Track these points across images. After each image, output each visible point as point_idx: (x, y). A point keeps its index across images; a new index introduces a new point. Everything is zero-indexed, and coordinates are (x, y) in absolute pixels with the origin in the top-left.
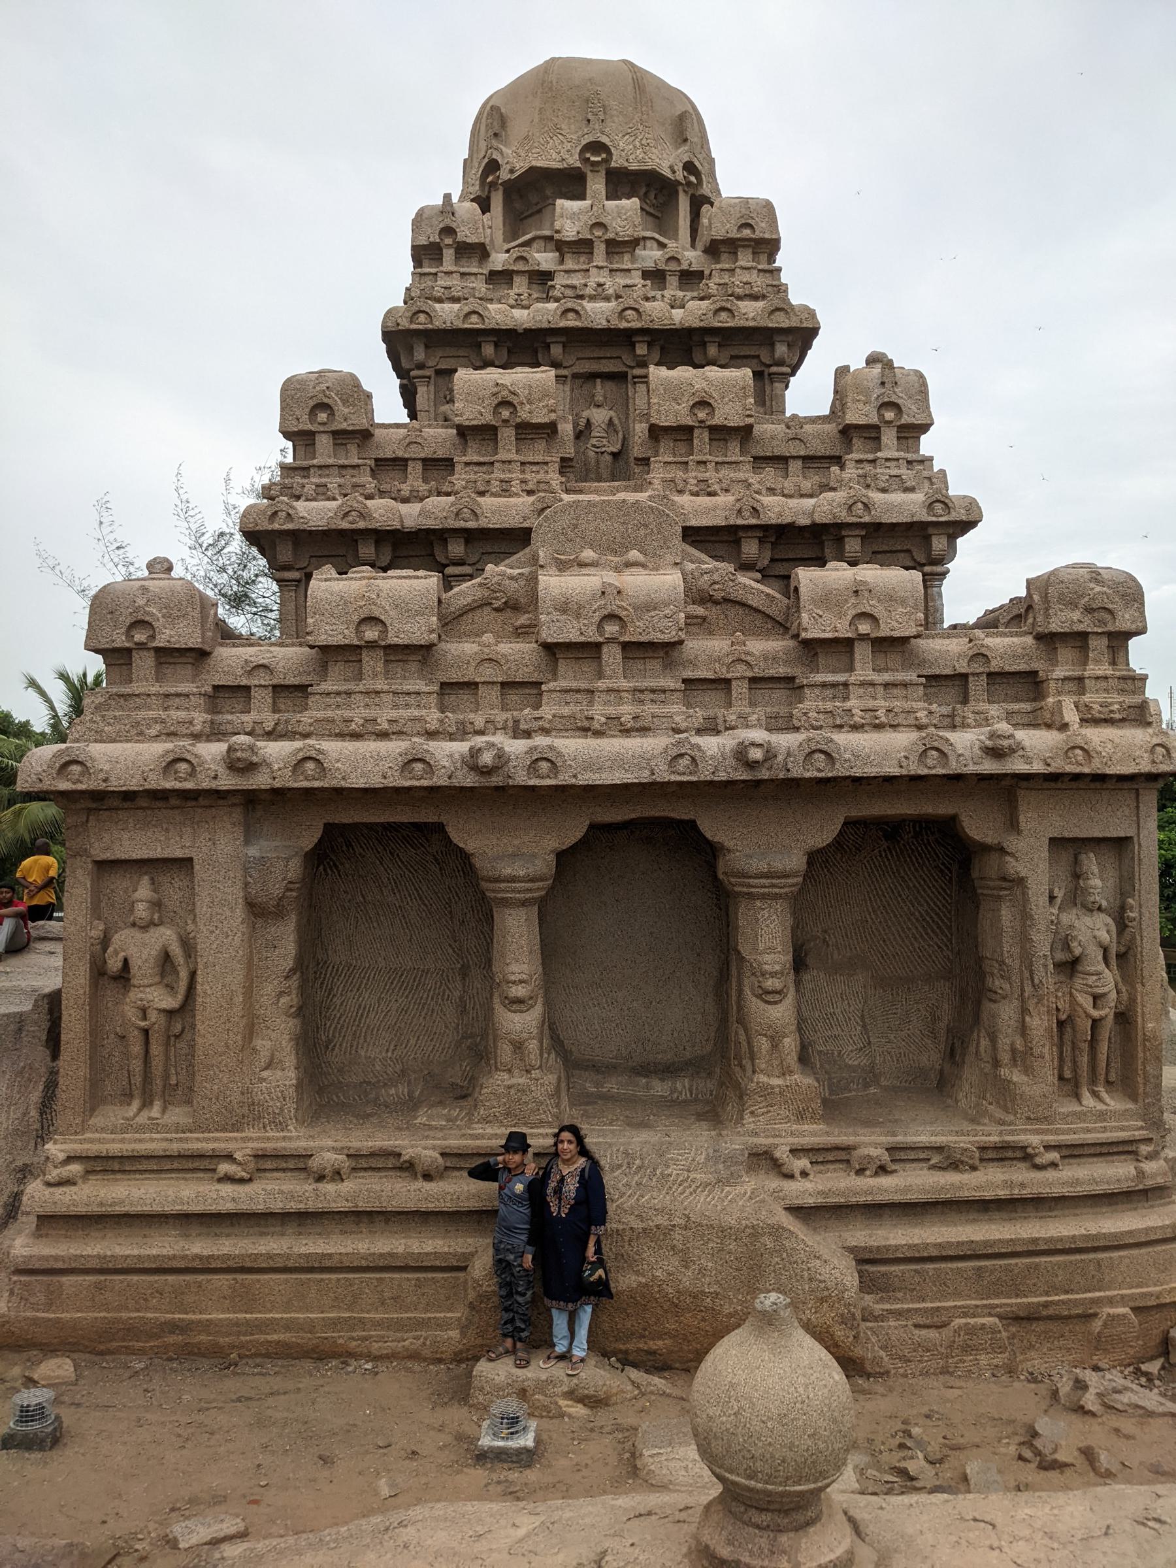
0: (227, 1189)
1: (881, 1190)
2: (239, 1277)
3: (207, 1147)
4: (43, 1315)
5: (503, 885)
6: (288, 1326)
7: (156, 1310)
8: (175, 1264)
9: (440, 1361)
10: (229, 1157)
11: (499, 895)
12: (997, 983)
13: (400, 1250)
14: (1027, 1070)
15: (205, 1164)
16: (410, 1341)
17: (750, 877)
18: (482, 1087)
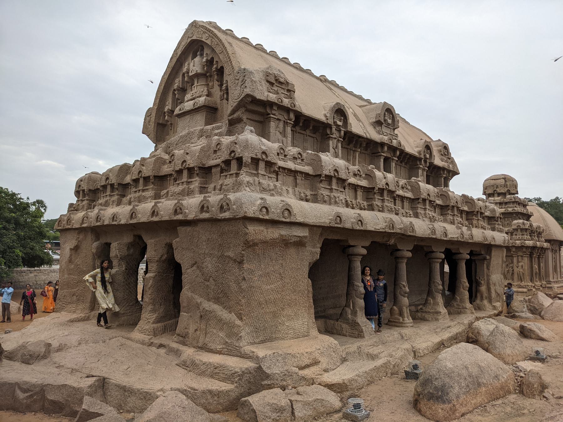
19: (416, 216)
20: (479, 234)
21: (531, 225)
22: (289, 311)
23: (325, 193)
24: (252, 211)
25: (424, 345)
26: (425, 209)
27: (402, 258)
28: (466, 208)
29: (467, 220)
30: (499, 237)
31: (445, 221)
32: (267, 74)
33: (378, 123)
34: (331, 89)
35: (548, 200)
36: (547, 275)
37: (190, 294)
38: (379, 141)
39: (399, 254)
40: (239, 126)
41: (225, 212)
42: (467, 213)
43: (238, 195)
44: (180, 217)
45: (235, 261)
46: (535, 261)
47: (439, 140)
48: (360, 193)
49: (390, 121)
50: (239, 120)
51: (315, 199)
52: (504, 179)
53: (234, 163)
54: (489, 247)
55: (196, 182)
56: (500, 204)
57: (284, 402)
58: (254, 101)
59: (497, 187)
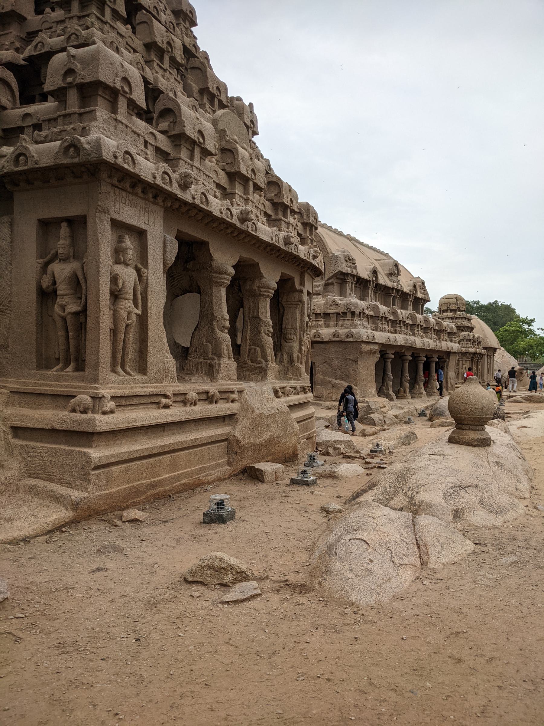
0: (167, 411)
1: (291, 401)
2: (172, 455)
3: (158, 390)
4: (105, 492)
5: (226, 276)
6: (186, 475)
7: (145, 478)
8: (155, 451)
9: (225, 479)
10: (165, 396)
11: (223, 281)
12: (292, 336)
13: (213, 434)
14: (301, 364)
15: (155, 400)
16: (216, 473)
17: (270, 289)
18: (219, 364)
19: (414, 335)
20: (446, 345)
21: (474, 336)
22: (369, 385)
23: (380, 325)
24: (364, 338)
25: (420, 407)
26: (418, 331)
27: (407, 360)
28: (437, 328)
29: (437, 335)
30: (455, 346)
31: (427, 337)
32: (345, 256)
33: (390, 274)
34: (357, 247)
35: (486, 304)
36: (483, 376)
37: (322, 377)
38: (391, 287)
39: (405, 358)
40: (331, 287)
41: (350, 338)
42: (437, 331)
43: (357, 330)
44: (318, 339)
45: (353, 361)
46: (475, 364)
47: (419, 277)
48: (390, 323)
49: (396, 272)
50: (332, 284)
51: (376, 329)
52: (456, 298)
53: (349, 313)
54: (448, 354)
55: (321, 322)
56: (452, 318)
57: (381, 418)
58: (342, 273)
59: (450, 305)
